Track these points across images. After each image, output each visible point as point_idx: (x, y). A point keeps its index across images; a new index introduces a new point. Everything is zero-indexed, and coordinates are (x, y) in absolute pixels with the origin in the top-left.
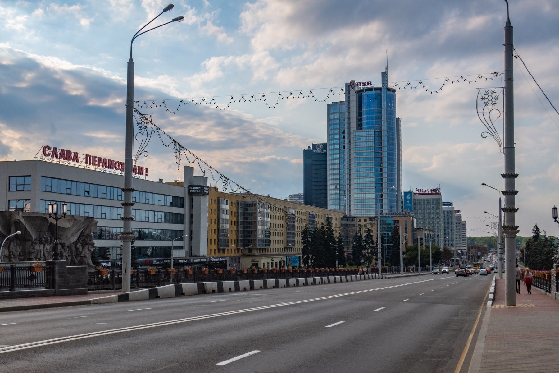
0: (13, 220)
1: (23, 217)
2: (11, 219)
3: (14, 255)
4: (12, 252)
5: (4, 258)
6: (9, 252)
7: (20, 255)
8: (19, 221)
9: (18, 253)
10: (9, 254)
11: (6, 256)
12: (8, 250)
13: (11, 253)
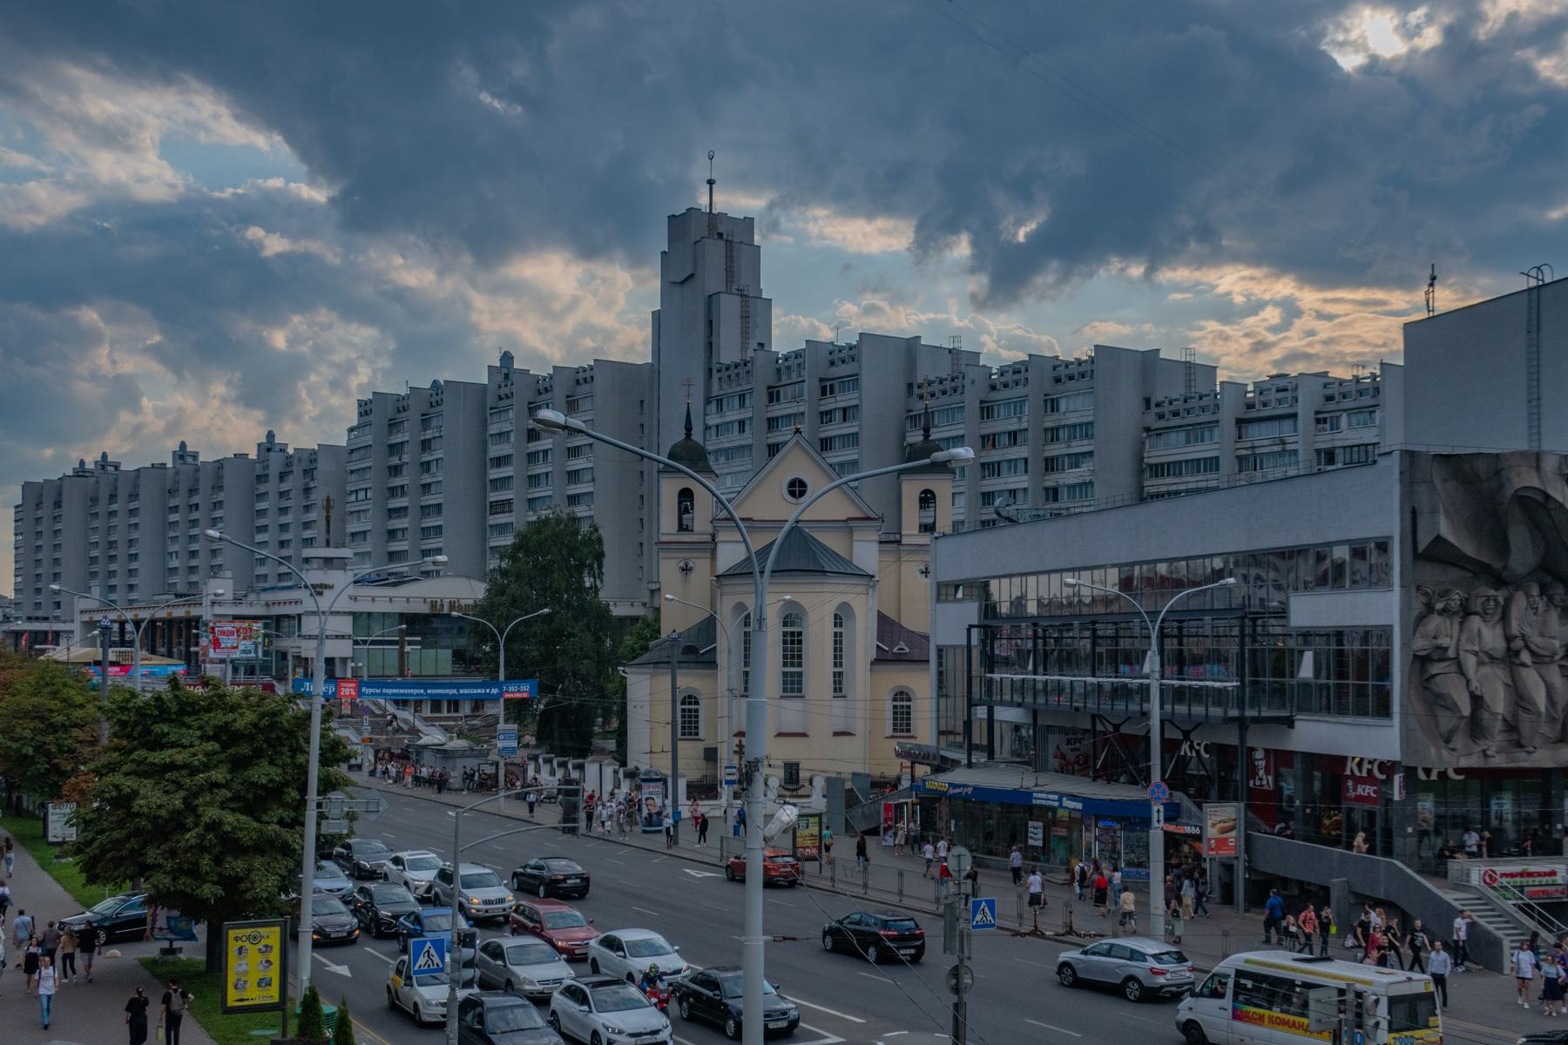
0: (1509, 492)
2: (1501, 486)
3: (1533, 653)
4: (1523, 637)
5: (1480, 663)
6: (1509, 639)
8: (1540, 498)
9: (1557, 643)
10: (1509, 649)
11: (1493, 659)
12: (1499, 630)
13: (1518, 644)
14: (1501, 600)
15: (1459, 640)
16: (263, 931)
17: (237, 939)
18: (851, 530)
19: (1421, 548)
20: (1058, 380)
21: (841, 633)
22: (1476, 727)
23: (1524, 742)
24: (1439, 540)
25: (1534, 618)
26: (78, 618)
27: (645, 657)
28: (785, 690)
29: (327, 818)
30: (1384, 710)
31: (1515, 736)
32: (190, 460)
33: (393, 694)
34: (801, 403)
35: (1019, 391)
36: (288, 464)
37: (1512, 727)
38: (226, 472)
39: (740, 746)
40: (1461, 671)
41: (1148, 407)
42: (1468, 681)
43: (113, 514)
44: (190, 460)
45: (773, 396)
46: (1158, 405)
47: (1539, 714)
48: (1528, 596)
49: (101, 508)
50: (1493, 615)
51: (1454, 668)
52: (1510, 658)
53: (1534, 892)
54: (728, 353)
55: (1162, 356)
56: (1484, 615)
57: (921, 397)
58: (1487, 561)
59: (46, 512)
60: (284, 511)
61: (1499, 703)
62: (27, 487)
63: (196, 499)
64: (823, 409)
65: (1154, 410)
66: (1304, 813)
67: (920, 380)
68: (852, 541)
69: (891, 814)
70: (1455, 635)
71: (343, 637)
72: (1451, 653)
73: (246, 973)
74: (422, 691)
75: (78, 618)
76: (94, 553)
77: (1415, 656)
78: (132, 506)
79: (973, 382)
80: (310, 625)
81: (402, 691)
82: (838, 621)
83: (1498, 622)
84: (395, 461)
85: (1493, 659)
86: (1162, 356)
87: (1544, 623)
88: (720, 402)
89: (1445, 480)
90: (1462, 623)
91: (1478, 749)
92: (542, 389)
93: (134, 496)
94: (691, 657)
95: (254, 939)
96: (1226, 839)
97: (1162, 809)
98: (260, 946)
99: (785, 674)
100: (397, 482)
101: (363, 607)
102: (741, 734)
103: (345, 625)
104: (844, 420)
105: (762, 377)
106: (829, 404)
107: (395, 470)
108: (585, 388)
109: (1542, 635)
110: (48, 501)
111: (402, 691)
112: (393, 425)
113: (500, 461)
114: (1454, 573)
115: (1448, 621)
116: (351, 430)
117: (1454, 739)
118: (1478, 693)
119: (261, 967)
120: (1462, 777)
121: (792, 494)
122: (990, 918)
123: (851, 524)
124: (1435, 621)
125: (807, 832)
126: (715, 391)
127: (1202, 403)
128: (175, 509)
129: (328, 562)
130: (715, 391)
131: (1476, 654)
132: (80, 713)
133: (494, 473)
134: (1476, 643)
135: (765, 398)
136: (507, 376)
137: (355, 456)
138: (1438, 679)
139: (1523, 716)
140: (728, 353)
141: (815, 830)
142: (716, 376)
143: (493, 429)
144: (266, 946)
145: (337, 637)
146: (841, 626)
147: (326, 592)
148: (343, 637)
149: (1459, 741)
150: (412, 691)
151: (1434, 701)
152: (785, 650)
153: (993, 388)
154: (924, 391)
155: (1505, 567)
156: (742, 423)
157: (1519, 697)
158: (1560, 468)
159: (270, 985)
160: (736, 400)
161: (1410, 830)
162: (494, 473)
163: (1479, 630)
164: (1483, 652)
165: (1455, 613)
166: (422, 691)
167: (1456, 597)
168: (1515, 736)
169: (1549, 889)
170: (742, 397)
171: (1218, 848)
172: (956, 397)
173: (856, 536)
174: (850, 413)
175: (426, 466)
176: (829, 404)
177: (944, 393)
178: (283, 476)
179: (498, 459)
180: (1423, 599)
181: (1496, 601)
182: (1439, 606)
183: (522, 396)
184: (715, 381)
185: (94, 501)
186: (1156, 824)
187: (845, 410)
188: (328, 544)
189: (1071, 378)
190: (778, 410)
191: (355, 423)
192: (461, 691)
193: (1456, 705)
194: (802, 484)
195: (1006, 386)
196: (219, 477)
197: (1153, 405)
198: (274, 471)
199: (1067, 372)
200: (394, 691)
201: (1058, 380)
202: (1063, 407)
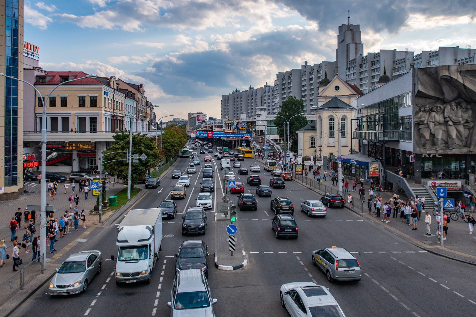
1: (460, 72)
3: (453, 122)
4: (449, 117)
5: (435, 125)
6: (445, 118)
7: (467, 122)
11: (440, 124)
12: (441, 116)
14: (442, 107)
15: (428, 119)
18: (350, 98)
19: (416, 93)
20: (430, 57)
21: (344, 122)
22: (434, 144)
23: (449, 147)
24: (419, 91)
25: (453, 112)
26: (224, 123)
27: (303, 129)
28: (330, 136)
30: (411, 139)
31: (447, 145)
32: (252, 89)
34: (366, 67)
35: (420, 60)
36: (270, 89)
37: (446, 143)
38: (258, 92)
39: (320, 149)
40: (429, 127)
41: (456, 62)
42: (431, 130)
43: (238, 101)
44: (252, 89)
45: (361, 66)
46: (459, 61)
47: (453, 139)
48: (451, 106)
49: (236, 100)
50: (440, 111)
51: (427, 126)
52: (446, 123)
53: (449, 189)
54: (352, 57)
55: (460, 48)
56: (437, 112)
57: (397, 64)
58: (438, 96)
59: (226, 101)
60: (269, 99)
61: (440, 135)
62: (223, 96)
63: (252, 98)
64: (372, 69)
65: (458, 62)
66: (403, 166)
67: (396, 59)
68: (350, 100)
69: (332, 165)
70: (427, 118)
71: (264, 126)
72: (425, 122)
75: (224, 123)
76: (235, 110)
77: (415, 124)
78: (241, 99)
79: (408, 59)
80: (258, 123)
82: (343, 119)
83: (441, 113)
84: (283, 87)
85: (440, 124)
86: (460, 48)
87: (457, 113)
88: (349, 69)
89: (423, 75)
90: (429, 114)
91: (433, 148)
92: (312, 68)
93: (241, 97)
94: (313, 128)
96: (375, 172)
97: (341, 163)
99: (330, 132)
100: (284, 92)
101: (269, 119)
102: (321, 146)
103: (265, 123)
104: (377, 71)
105: (358, 62)
106: (373, 68)
107: (283, 89)
108: (321, 68)
109: (456, 117)
110: (227, 99)
112: (283, 79)
113: (304, 86)
114: (429, 101)
115: (425, 114)
116: (275, 81)
117: (426, 146)
118: (433, 133)
120: (441, 157)
121: (336, 89)
123: (350, 96)
124: (421, 113)
125: (299, 168)
126: (349, 67)
127: (470, 59)
128: (249, 100)
129: (261, 110)
130: (349, 67)
131: (434, 122)
132: (169, 140)
133: (303, 89)
134: (434, 119)
135: (359, 67)
136: (306, 67)
137: (276, 87)
138: (421, 129)
139: (449, 139)
140: (352, 57)
141: (301, 168)
142: (349, 63)
143: (303, 79)
145: (263, 126)
146: (344, 120)
147: (260, 116)
148: (264, 126)
149: (428, 146)
151: (421, 136)
152: (330, 126)
153: (414, 60)
154: (398, 62)
155: (444, 98)
156: (354, 74)
157: (449, 135)
158: (457, 69)
160: (352, 68)
161: (417, 170)
162: (303, 89)
163: (434, 116)
164: (437, 122)
165: (428, 111)
167: (427, 108)
168: (447, 145)
169: (455, 188)
170: (354, 67)
171: (373, 174)
172: (405, 63)
173: (351, 99)
174: (378, 69)
175: (289, 88)
176: (373, 68)
177: (402, 63)
178: (269, 92)
179: (304, 85)
180: (418, 108)
181: (440, 107)
182: (422, 109)
183: (308, 71)
184: (349, 64)
185: (235, 98)
186: (339, 167)
187: (377, 69)
188: (261, 106)
189: (434, 56)
190: (362, 70)
191: (276, 79)
193: (425, 136)
194: (338, 87)
195: (417, 59)
196: (257, 93)
197: (457, 60)
198: (267, 91)
199: (433, 54)
201: (430, 57)
202: (431, 64)
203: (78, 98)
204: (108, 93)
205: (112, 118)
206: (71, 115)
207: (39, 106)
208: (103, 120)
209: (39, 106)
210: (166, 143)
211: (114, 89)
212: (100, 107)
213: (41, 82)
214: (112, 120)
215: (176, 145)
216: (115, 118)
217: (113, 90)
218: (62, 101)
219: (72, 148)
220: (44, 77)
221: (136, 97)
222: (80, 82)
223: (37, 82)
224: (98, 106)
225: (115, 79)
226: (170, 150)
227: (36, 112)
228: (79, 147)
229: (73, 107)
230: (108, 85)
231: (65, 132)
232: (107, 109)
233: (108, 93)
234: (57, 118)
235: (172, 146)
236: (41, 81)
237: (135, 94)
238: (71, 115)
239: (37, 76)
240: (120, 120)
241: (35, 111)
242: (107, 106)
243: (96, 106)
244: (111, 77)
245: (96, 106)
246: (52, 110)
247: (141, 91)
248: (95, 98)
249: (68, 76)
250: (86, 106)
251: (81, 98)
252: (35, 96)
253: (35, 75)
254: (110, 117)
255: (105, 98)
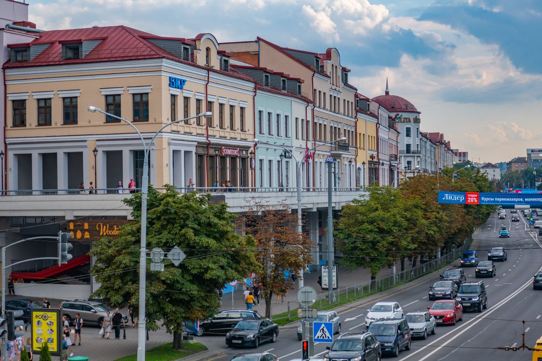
16: (49, 314)
17: (37, 316)
29: (152, 262)
33: (502, 202)
73: (41, 334)
74: (521, 200)
81: (508, 200)
95: (45, 318)
98: (48, 321)
111: (508, 200)
119: (48, 332)
122: (328, 334)
132: (372, 215)
144: (50, 322)
150: (515, 199)
159: (53, 342)
166: (521, 200)
192: (493, 199)
200: (503, 199)
203: (103, 99)
204: (183, 82)
205: (201, 151)
206: (86, 147)
207: (15, 125)
208: (167, 158)
209: (15, 125)
210: (363, 222)
211: (209, 69)
212: (157, 121)
213: (20, 62)
214: (200, 157)
215: (395, 229)
216: (212, 152)
217: (204, 73)
218: (65, 107)
219: (83, 237)
220: (25, 47)
221: (306, 90)
222: (109, 56)
223: (9, 61)
224: (151, 120)
225: (212, 39)
226: (374, 244)
227: (8, 141)
228: (99, 231)
229: (92, 123)
230: (186, 59)
231: (47, 193)
232: (181, 127)
233: (183, 82)
234: (30, 155)
235: (381, 231)
236: (19, 58)
237: (298, 80)
238: (86, 147)
239: (9, 46)
240: (233, 159)
241: (5, 138)
242: (180, 115)
243: (75, 122)
244: (200, 37)
245: (146, 118)
246: (44, 131)
247: (328, 69)
248: (144, 99)
249: (80, 42)
250: (53, 125)
251: (110, 100)
252: (6, 97)
253: (5, 44)
254: (193, 150)
255: (173, 97)
